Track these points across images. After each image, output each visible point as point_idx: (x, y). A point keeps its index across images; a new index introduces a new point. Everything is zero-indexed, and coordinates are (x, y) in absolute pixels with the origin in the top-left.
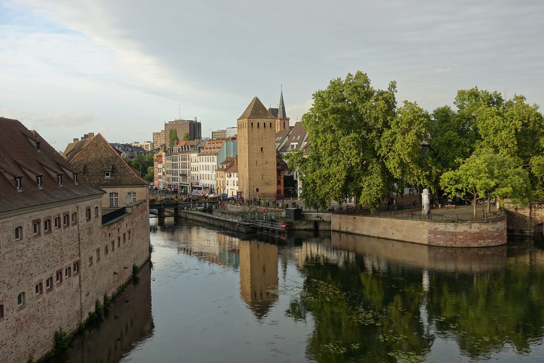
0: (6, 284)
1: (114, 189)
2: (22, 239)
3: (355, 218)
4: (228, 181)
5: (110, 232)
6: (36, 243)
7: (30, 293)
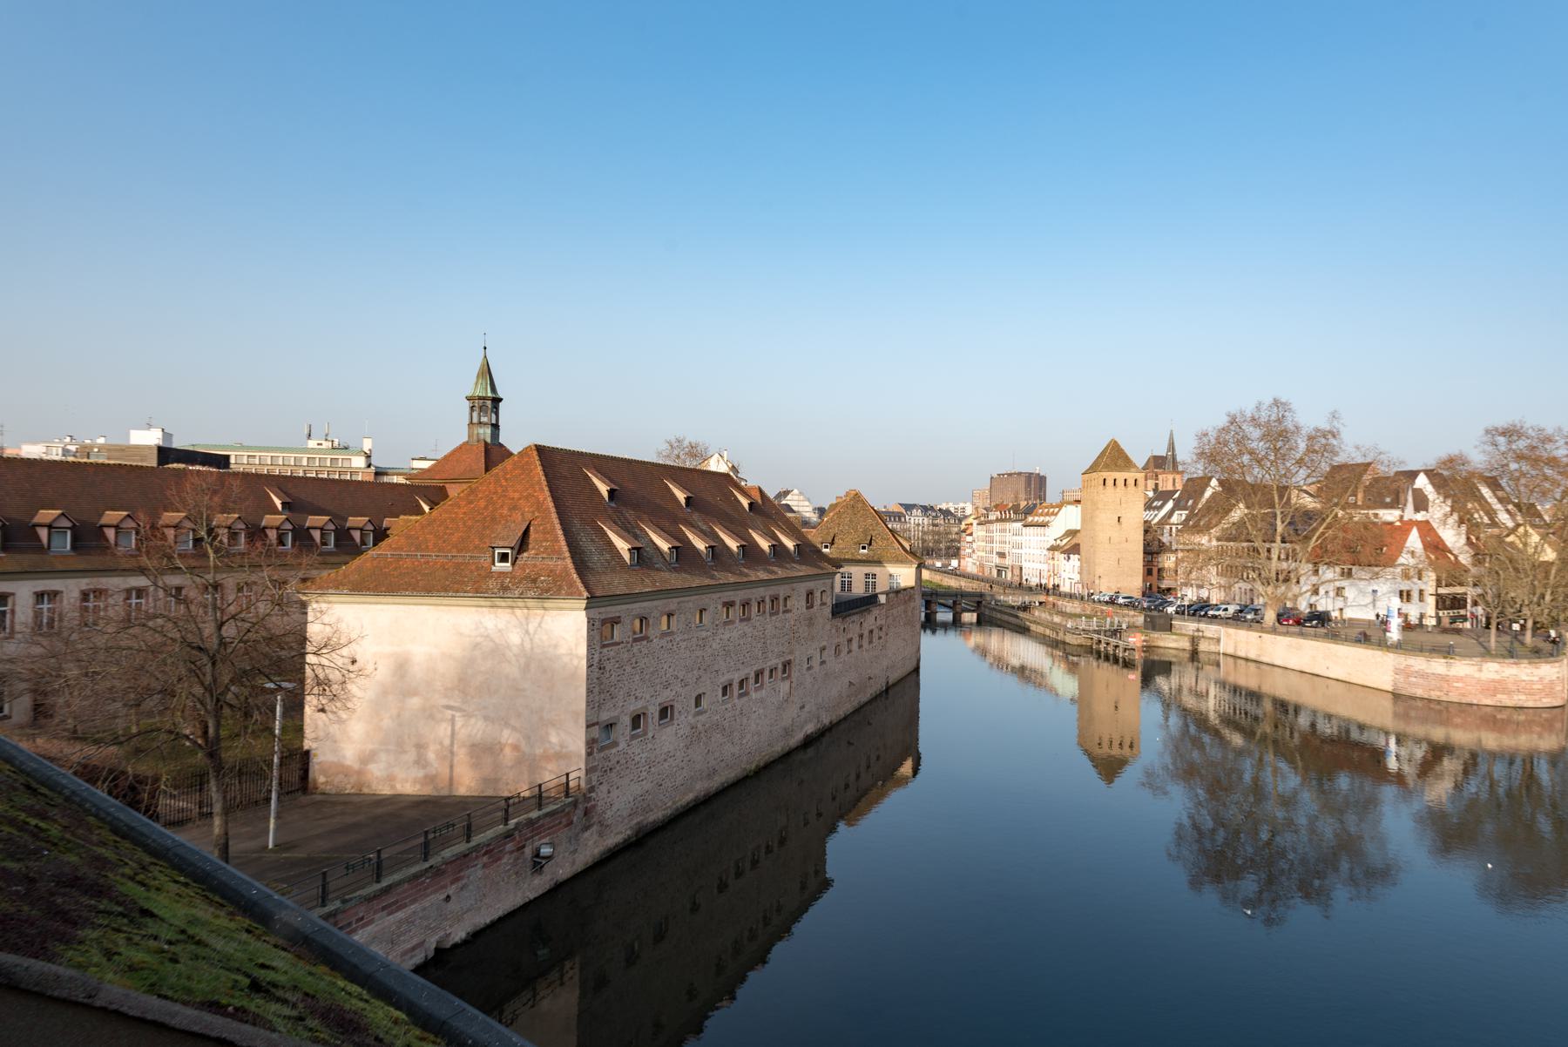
3: (1260, 637)
7: (712, 697)
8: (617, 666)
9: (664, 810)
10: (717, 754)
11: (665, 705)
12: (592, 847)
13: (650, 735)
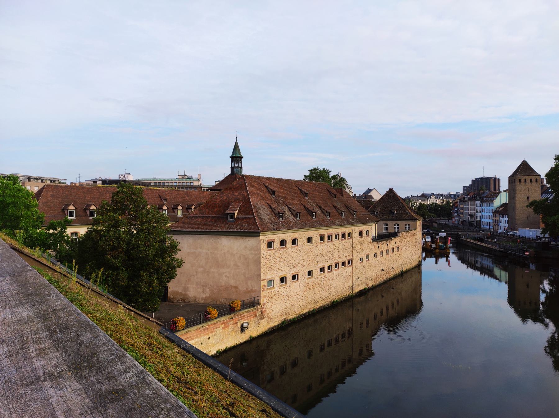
0: (301, 264)
2: (312, 243)
4: (501, 220)
5: (379, 246)
6: (321, 246)
7: (316, 272)
8: (273, 258)
9: (295, 315)
10: (318, 295)
11: (295, 274)
13: (288, 285)
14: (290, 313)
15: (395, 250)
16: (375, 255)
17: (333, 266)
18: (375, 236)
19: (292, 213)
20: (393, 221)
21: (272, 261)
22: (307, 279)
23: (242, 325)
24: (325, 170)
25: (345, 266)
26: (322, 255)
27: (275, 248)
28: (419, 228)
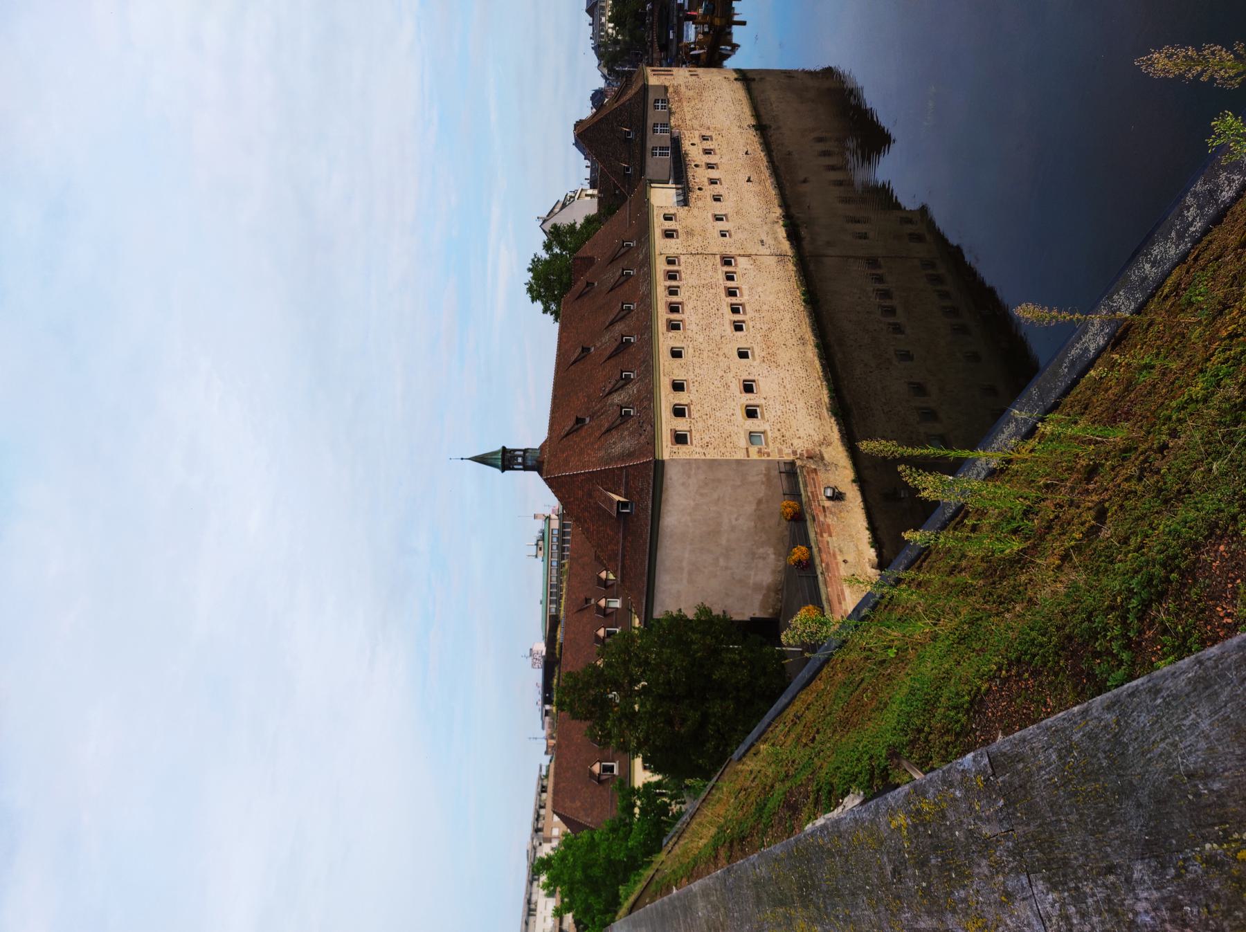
1: (648, 129)
2: (683, 348)
6: (691, 327)
7: (741, 340)
10: (788, 336)
11: (742, 387)
12: (837, 453)
13: (762, 402)
14: (818, 398)
15: (708, 145)
16: (717, 199)
17: (734, 300)
18: (676, 188)
19: (622, 387)
20: (646, 135)
21: (713, 434)
22: (754, 359)
23: (829, 498)
24: (531, 267)
25: (735, 273)
26: (708, 326)
27: (688, 429)
28: (663, 77)
